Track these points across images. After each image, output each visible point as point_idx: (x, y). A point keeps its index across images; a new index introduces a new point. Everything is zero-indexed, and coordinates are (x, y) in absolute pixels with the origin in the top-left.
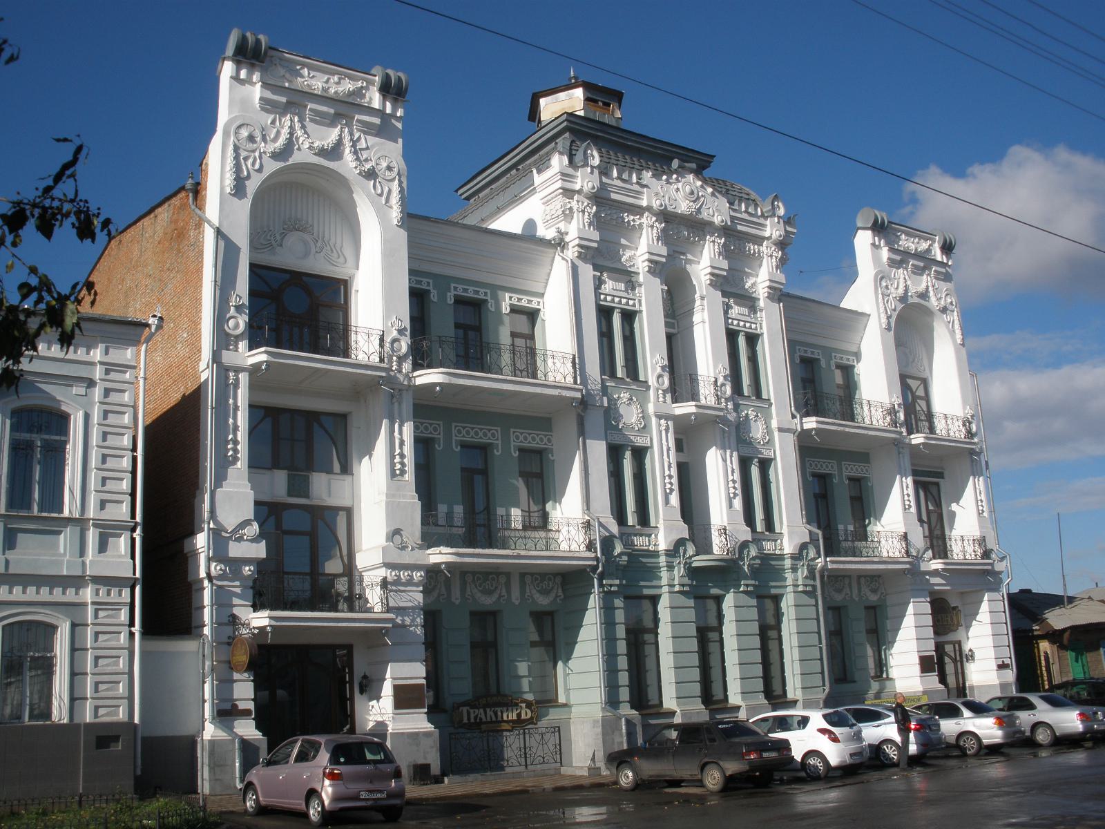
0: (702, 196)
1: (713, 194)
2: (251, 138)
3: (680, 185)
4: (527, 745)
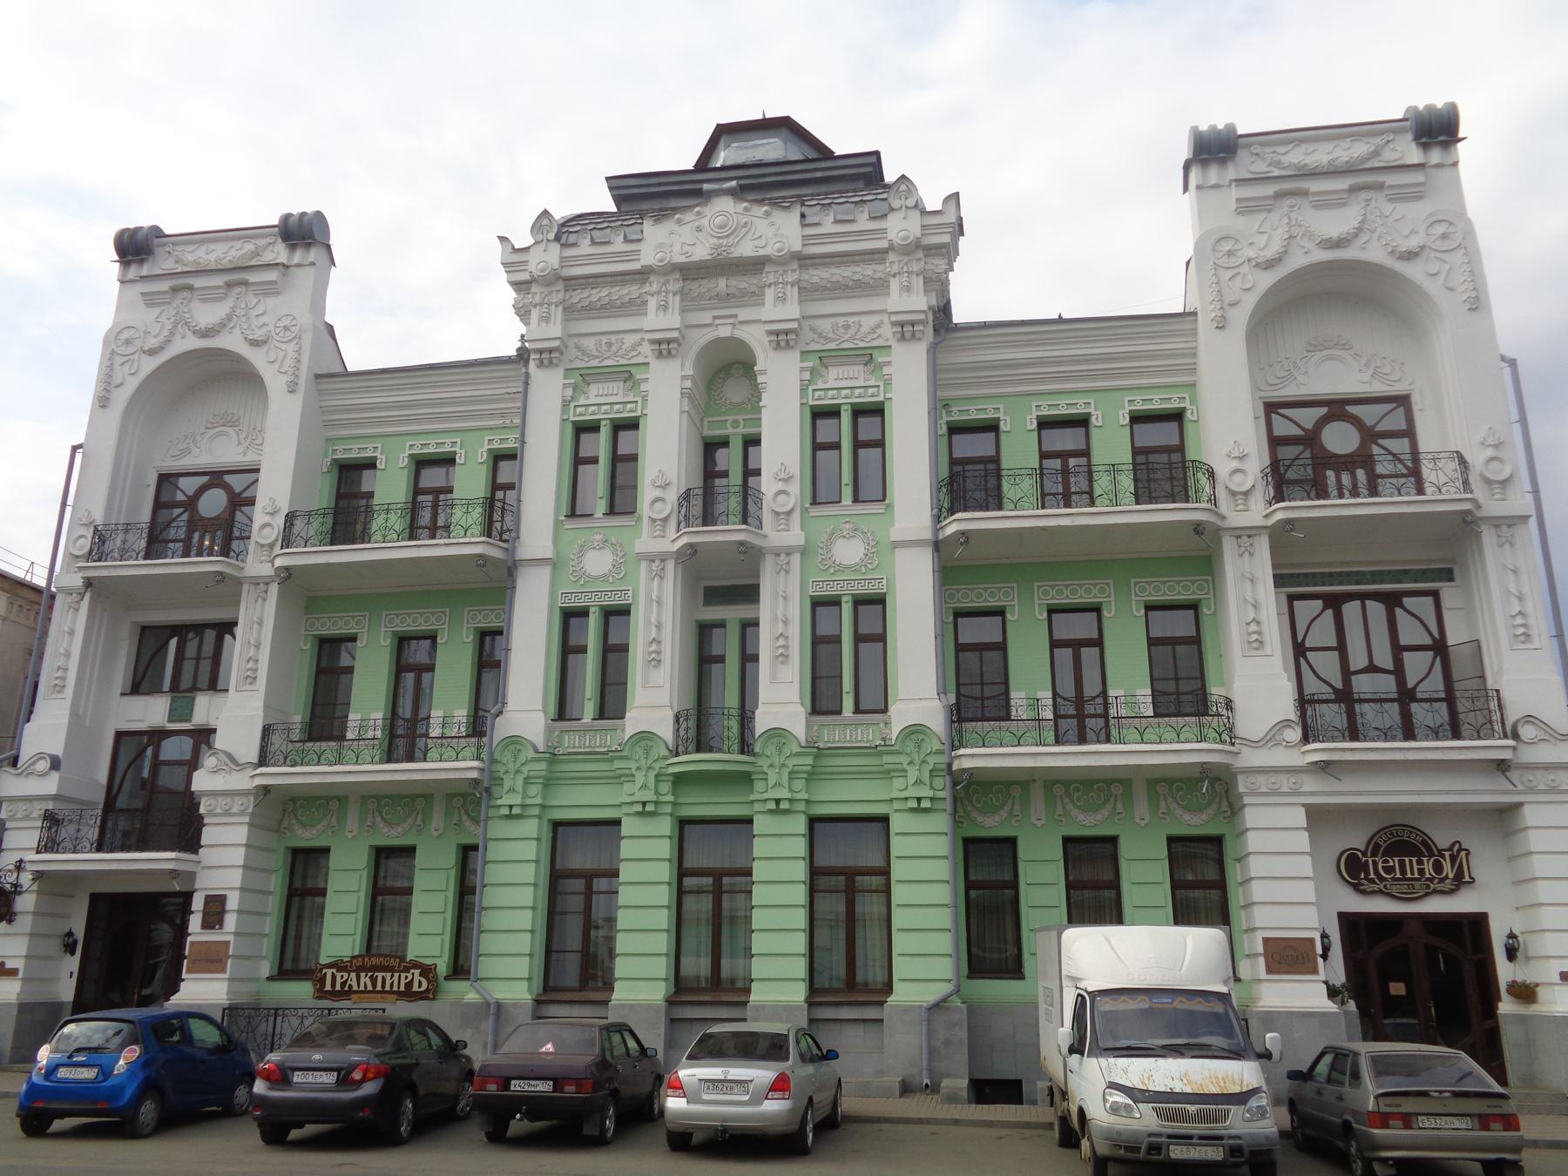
0: (746, 223)
2: (128, 342)
3: (705, 222)
4: (278, 1031)
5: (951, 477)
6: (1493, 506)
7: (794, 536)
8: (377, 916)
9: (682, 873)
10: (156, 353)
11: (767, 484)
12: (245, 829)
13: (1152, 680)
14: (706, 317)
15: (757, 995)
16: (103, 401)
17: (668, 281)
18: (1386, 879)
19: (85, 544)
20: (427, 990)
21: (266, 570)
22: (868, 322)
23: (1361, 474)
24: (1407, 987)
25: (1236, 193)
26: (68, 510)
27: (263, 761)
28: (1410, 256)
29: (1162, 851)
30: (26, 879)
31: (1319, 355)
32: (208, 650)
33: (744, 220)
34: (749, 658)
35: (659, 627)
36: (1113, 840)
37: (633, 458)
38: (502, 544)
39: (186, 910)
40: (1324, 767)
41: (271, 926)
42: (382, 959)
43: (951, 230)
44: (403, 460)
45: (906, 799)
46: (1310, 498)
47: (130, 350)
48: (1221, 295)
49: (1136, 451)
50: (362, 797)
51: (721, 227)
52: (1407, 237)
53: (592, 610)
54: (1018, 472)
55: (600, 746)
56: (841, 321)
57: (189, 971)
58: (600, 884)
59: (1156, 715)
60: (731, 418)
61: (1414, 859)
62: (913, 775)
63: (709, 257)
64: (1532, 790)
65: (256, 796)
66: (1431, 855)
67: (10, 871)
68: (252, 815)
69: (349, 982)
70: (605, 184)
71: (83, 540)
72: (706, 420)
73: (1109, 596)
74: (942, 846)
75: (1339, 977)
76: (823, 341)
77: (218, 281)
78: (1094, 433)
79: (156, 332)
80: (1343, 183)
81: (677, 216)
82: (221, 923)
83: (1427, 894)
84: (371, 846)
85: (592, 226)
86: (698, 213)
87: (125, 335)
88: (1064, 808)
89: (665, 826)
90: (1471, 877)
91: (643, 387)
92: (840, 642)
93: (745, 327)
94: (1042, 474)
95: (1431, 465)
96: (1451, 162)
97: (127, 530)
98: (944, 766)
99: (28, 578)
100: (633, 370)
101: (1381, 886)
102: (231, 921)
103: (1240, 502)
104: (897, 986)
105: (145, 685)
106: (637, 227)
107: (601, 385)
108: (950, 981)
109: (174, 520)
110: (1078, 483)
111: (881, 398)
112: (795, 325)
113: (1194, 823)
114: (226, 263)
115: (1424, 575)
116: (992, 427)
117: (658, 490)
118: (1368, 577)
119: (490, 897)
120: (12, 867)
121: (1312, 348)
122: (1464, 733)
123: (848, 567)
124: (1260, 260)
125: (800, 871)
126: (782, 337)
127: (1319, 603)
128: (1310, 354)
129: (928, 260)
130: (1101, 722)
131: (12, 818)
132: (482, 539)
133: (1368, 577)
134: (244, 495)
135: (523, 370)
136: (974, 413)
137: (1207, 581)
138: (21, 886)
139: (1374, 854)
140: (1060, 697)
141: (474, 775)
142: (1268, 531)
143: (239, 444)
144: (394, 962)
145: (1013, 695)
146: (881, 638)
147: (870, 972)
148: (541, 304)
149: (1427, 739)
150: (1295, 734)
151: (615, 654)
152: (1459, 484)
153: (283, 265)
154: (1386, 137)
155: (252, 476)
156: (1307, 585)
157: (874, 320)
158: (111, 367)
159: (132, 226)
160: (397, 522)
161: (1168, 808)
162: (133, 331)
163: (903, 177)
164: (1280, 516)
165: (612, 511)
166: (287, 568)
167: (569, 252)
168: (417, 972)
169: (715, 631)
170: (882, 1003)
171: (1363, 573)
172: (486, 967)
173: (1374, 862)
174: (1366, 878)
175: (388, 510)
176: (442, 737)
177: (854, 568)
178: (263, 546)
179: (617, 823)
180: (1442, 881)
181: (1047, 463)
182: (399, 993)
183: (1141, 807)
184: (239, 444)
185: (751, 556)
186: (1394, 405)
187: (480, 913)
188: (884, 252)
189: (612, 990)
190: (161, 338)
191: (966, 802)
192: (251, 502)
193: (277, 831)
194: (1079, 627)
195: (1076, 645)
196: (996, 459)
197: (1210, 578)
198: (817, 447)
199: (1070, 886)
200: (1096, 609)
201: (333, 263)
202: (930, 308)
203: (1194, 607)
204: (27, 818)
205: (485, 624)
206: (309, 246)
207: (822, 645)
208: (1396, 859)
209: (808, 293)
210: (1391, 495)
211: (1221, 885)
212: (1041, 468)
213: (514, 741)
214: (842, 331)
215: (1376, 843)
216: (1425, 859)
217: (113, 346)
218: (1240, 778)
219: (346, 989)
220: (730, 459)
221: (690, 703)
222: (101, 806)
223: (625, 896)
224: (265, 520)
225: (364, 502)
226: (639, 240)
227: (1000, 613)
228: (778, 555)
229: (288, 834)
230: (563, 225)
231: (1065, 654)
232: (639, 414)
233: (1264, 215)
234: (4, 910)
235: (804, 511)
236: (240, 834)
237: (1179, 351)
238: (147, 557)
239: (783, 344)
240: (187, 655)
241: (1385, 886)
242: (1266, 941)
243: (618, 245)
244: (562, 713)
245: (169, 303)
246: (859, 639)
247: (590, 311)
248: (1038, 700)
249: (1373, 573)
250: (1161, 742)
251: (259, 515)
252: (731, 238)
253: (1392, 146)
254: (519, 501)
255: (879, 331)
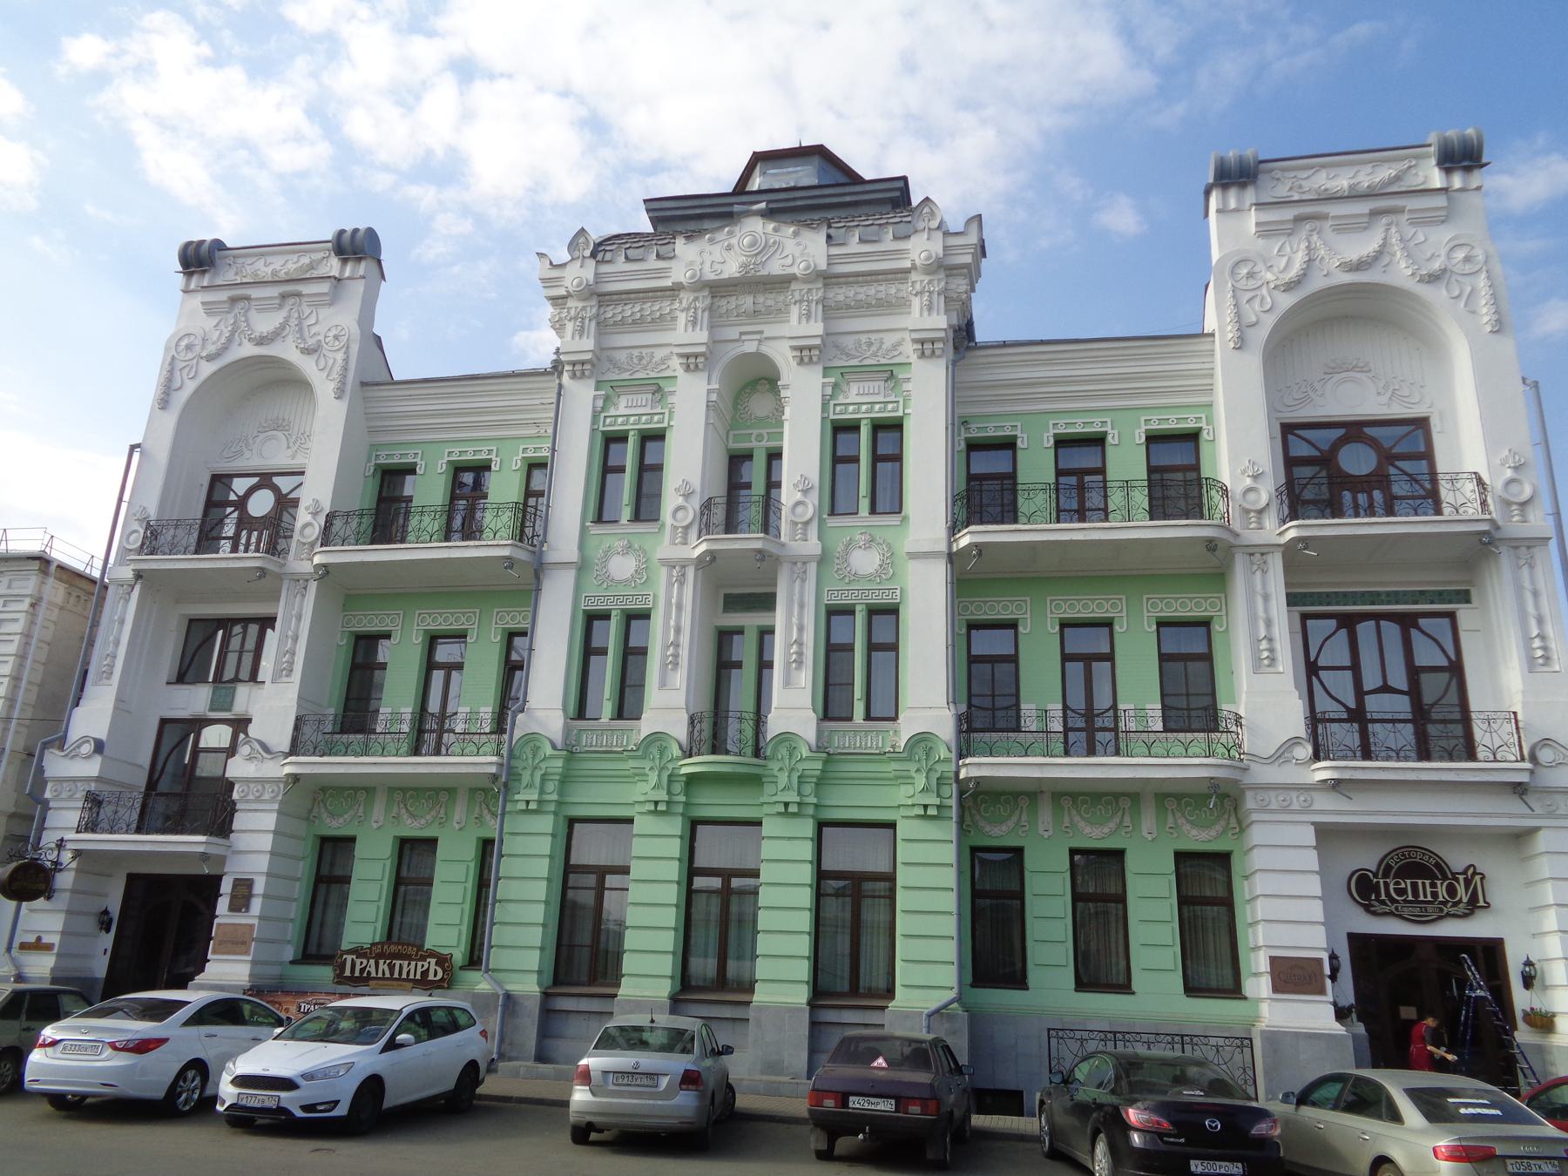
0: (774, 243)
1: (796, 234)
2: (189, 347)
3: (734, 241)
5: (968, 490)
6: (1514, 526)
7: (812, 546)
8: (399, 907)
9: (692, 871)
10: (213, 359)
11: (788, 495)
12: (274, 816)
13: (1163, 695)
14: (733, 333)
15: (761, 995)
16: (164, 402)
17: (696, 299)
18: (1397, 901)
19: (136, 541)
20: (442, 979)
21: (306, 567)
22: (890, 340)
23: (1377, 495)
24: (1418, 1011)
25: (1252, 218)
26: (124, 506)
27: (294, 750)
28: (1433, 278)
29: (1170, 865)
30: (66, 856)
31: (1337, 377)
32: (250, 644)
33: (772, 241)
34: (764, 665)
35: (678, 630)
36: (1119, 855)
37: (659, 468)
38: (530, 548)
39: (217, 895)
40: (1336, 785)
41: (296, 911)
42: (400, 947)
43: (972, 251)
44: (441, 466)
45: (913, 805)
46: (1324, 517)
47: (190, 355)
48: (1239, 317)
49: (1151, 470)
50: (389, 788)
51: (753, 244)
52: (1428, 260)
53: (614, 613)
54: (1032, 487)
55: (617, 746)
56: (864, 338)
57: (214, 952)
58: (611, 880)
59: (1166, 730)
60: (755, 432)
61: (1427, 882)
62: (921, 781)
63: (738, 275)
64: (1551, 815)
65: (286, 783)
66: (1445, 878)
67: (52, 849)
68: (281, 802)
69: (368, 969)
70: (643, 207)
71: (134, 535)
72: (731, 433)
73: (1121, 611)
74: (949, 853)
75: (1349, 998)
76: (844, 357)
77: (273, 291)
78: (1110, 451)
79: (215, 339)
80: (1363, 208)
81: (707, 236)
82: (247, 907)
83: (1440, 918)
84: (395, 837)
85: (628, 246)
86: (730, 233)
87: (183, 343)
88: (1071, 820)
89: (675, 826)
90: (1485, 902)
91: (670, 399)
92: (853, 650)
93: (771, 343)
94: (1057, 490)
95: (1449, 486)
96: (1475, 186)
97: (177, 525)
98: (952, 775)
99: (88, 571)
100: (661, 383)
101: (1393, 908)
102: (256, 905)
103: (1253, 519)
104: (899, 991)
105: (189, 677)
106: (671, 246)
107: (630, 397)
108: (952, 988)
109: (227, 516)
110: (1094, 499)
111: (900, 413)
112: (818, 341)
113: (1199, 839)
114: (282, 275)
115: (1440, 596)
116: (1009, 445)
117: (681, 498)
118: (1383, 597)
119: (504, 890)
120: (53, 845)
121: (1331, 371)
122: (1480, 755)
123: (864, 577)
124: (1278, 283)
125: (806, 874)
126: (806, 353)
127: (1333, 623)
128: (1328, 377)
129: (951, 280)
130: (1109, 736)
131: (57, 798)
132: (510, 542)
133: (1383, 597)
134: (291, 496)
135: (557, 382)
136: (992, 431)
137: (1219, 598)
138: (61, 864)
139: (1386, 875)
140: (1071, 709)
141: (493, 770)
142: (1281, 549)
143: (288, 447)
144: (411, 951)
145: (1023, 706)
146: (894, 647)
147: (871, 976)
148: (575, 318)
149: (1441, 759)
150: (1306, 751)
151: (633, 656)
152: (1477, 505)
153: (335, 278)
154: (1406, 164)
155: (297, 479)
156: (1321, 604)
157: (896, 337)
158: (171, 372)
159: (196, 239)
160: (434, 524)
161: (1176, 823)
162: (192, 338)
163: (927, 199)
164: (1292, 534)
165: (637, 517)
166: (325, 566)
167: (605, 268)
168: (433, 961)
169: (736, 637)
170: (883, 1008)
171: (1378, 594)
172: (496, 958)
173: (1385, 883)
174: (1377, 899)
175: (422, 512)
176: (464, 733)
177: (869, 578)
178: (304, 544)
179: (630, 821)
180: (1455, 904)
181: (1062, 480)
182: (415, 981)
183: (1148, 822)
184: (288, 447)
185: (768, 562)
186: (1411, 428)
187: (493, 905)
188: (907, 271)
189: (619, 985)
190: (219, 345)
191: (974, 812)
192: (295, 503)
193: (307, 819)
194: (1093, 642)
195: (1088, 659)
196: (1012, 476)
197: (1223, 595)
198: (837, 460)
199: (1076, 898)
200: (1108, 624)
201: (383, 277)
202: (950, 326)
203: (1206, 624)
204: (71, 798)
205: (513, 626)
206: (360, 259)
207: (834, 653)
208: (1408, 881)
209: (830, 311)
210: (1407, 515)
211: (1228, 903)
212: (1057, 483)
213: (531, 738)
214: (864, 348)
215: (1387, 864)
216: (1439, 882)
217: (173, 352)
218: (1249, 795)
219: (365, 975)
220: (755, 473)
221: (705, 705)
222: (143, 790)
223: (636, 893)
224: (306, 522)
225: (404, 505)
226: (671, 258)
227: (1012, 625)
228: (795, 563)
229: (317, 823)
230: (600, 244)
231: (1076, 668)
232: (665, 425)
233: (1282, 239)
234: (43, 887)
235: (821, 522)
236: (269, 820)
237: (1194, 372)
238: (196, 552)
239: (806, 359)
240: (231, 648)
241: (1396, 909)
242: (1273, 960)
243: (652, 263)
244: (581, 710)
245: (228, 312)
246: (872, 647)
247: (622, 325)
248: (1046, 711)
249: (1388, 594)
250: (1168, 756)
251: (303, 516)
252: (759, 257)
253: (1414, 172)
254: (548, 506)
255: (901, 348)
